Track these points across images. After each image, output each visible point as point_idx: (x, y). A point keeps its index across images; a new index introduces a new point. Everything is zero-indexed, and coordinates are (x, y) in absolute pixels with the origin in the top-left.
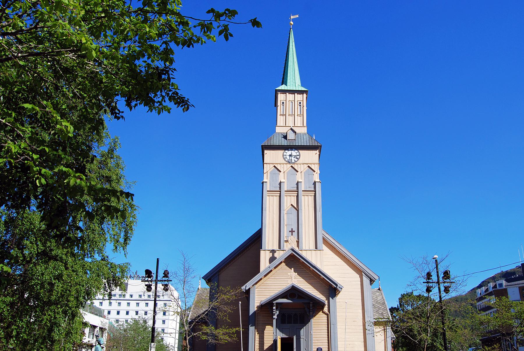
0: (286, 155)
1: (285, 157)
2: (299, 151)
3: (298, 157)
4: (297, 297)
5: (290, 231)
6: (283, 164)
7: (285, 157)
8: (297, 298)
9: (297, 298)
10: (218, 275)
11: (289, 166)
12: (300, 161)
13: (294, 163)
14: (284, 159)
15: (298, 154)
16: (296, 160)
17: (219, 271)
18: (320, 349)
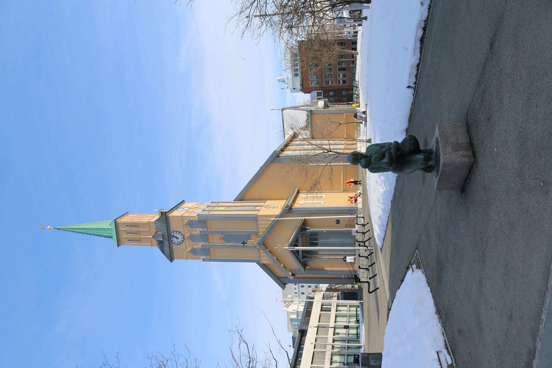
0: (177, 242)
1: (179, 243)
2: (172, 232)
3: (178, 232)
4: (297, 243)
5: (244, 245)
6: (186, 245)
7: (179, 243)
8: (298, 243)
9: (298, 243)
10: (281, 278)
11: (186, 240)
12: (182, 231)
13: (184, 236)
14: (181, 244)
15: (175, 232)
16: (180, 234)
17: (278, 278)
18: (337, 221)
